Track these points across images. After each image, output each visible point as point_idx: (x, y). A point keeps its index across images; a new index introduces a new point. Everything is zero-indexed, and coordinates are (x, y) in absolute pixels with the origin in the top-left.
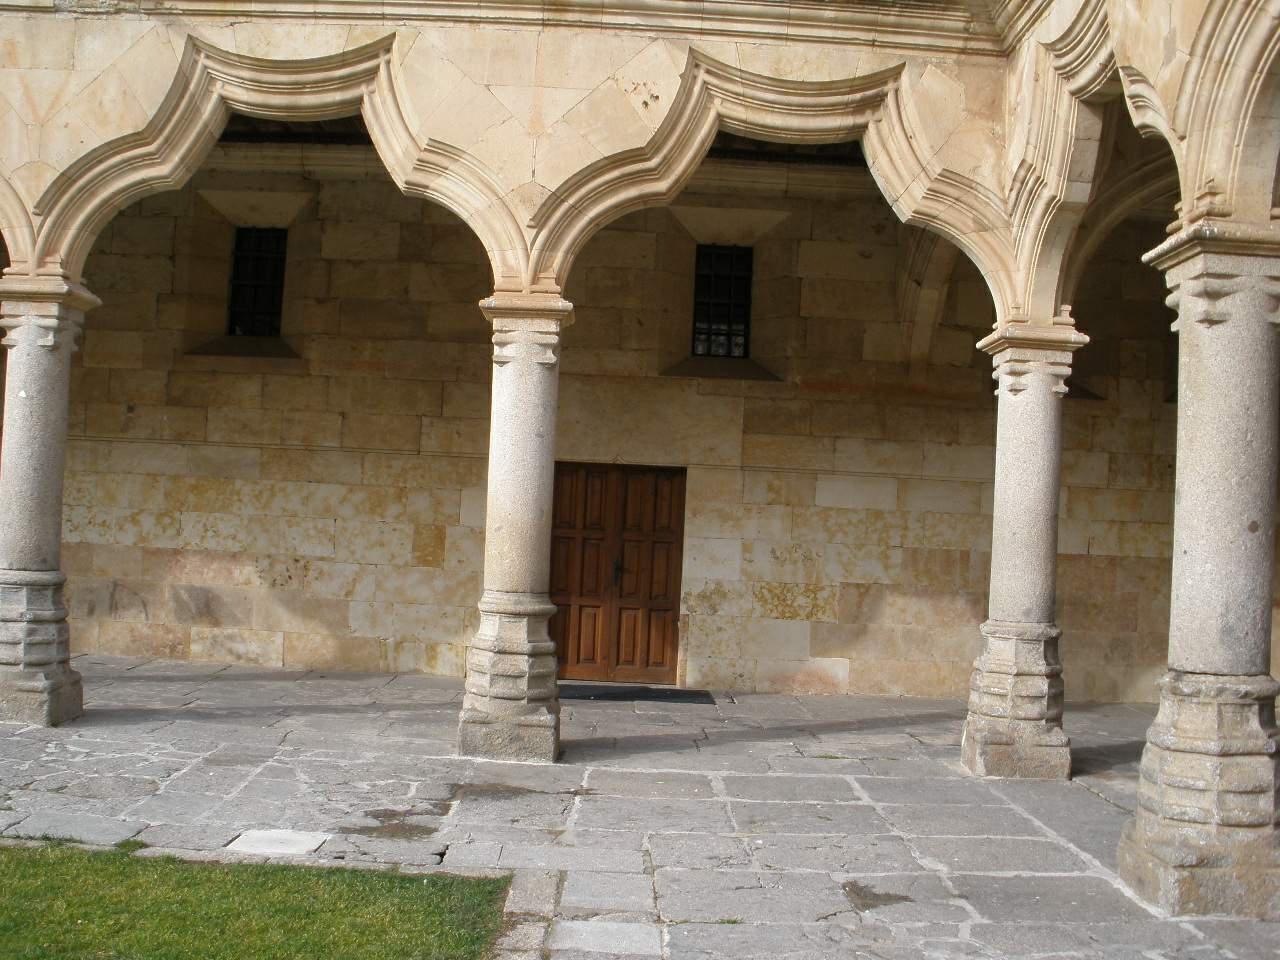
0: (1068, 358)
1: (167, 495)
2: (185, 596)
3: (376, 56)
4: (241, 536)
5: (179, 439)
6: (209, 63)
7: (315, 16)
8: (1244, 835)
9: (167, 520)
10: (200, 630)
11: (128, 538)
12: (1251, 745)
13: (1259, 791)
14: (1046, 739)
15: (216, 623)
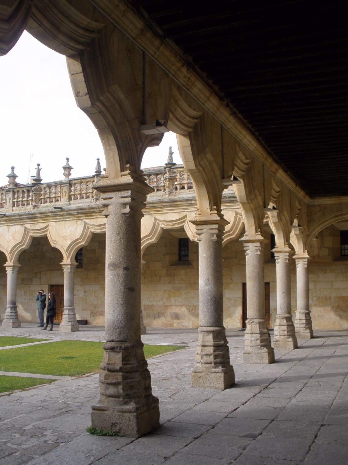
0: (307, 260)
1: (168, 294)
2: (172, 314)
3: (185, 218)
4: (183, 302)
5: (170, 283)
6: (158, 222)
7: (174, 212)
8: (283, 337)
9: (168, 299)
10: (176, 321)
11: (161, 303)
12: (284, 324)
13: (285, 331)
14: (306, 331)
15: (179, 319)
